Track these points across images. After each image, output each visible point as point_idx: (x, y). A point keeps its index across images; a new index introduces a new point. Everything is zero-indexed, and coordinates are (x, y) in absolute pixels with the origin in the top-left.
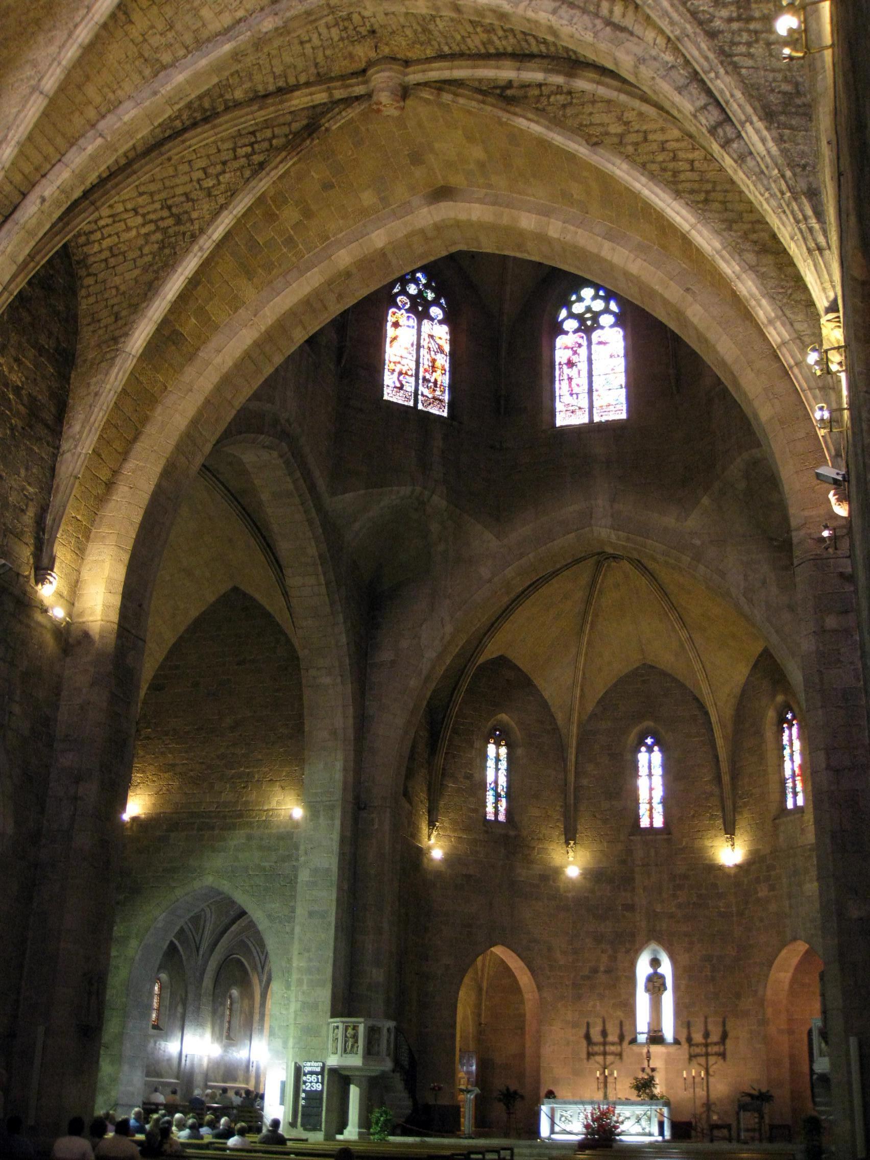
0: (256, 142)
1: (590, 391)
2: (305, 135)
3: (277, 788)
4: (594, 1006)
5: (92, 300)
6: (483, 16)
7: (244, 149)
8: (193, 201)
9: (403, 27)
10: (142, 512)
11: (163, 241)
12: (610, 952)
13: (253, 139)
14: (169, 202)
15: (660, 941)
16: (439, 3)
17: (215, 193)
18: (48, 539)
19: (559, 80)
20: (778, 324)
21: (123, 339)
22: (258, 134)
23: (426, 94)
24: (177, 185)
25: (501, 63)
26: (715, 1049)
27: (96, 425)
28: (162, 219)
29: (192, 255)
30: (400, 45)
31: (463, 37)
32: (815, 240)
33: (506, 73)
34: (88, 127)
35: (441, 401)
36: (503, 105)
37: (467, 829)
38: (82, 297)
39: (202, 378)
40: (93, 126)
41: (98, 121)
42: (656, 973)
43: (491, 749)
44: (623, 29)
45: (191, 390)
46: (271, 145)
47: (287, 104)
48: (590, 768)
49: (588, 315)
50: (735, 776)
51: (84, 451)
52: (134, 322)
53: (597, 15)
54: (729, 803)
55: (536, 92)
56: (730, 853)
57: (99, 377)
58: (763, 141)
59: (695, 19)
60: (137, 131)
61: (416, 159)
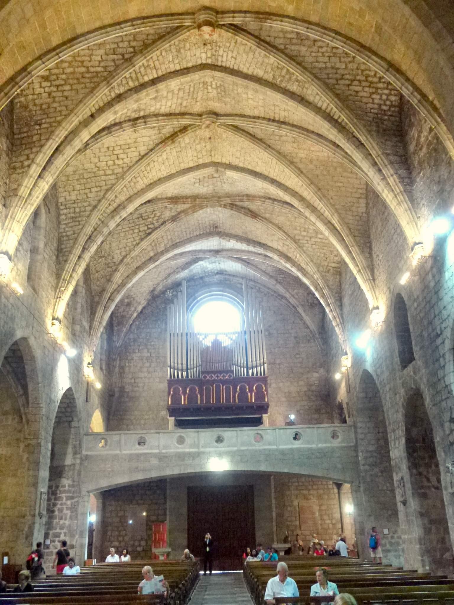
31: (161, 54)
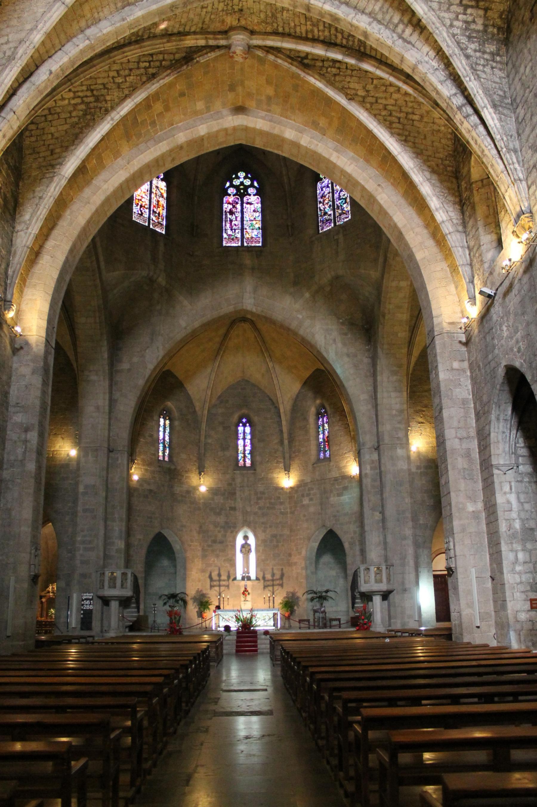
0: (152, 61)
1: (242, 229)
2: (183, 62)
3: (59, 439)
4: (214, 561)
5: (33, 139)
6: (323, 17)
7: (145, 64)
8: (108, 89)
9: (261, 11)
10: (58, 272)
11: (86, 110)
12: (222, 532)
13: (151, 59)
14: (92, 87)
15: (249, 526)
16: (298, 4)
17: (123, 87)
18: (10, 284)
19: (352, 61)
20: (441, 211)
21: (58, 167)
22: (154, 57)
23: (260, 53)
24: (99, 78)
25: (315, 44)
26: (278, 582)
27: (41, 217)
28: (87, 96)
29: (106, 122)
30: (253, 22)
31: (295, 25)
32: (517, 175)
33: (319, 51)
34: (79, 31)
35: (162, 225)
36: (303, 68)
37: (150, 464)
38: (27, 137)
39: (95, 197)
40: (82, 31)
41: (85, 29)
42: (246, 543)
43: (162, 421)
44: (409, 43)
45: (89, 203)
46: (161, 64)
47: (184, 42)
48: (212, 433)
49: (242, 187)
50: (291, 440)
51: (33, 232)
52: (66, 157)
53: (394, 31)
54: (287, 455)
55: (321, 64)
56: (287, 481)
57: (42, 188)
58: (493, 119)
59: (459, 46)
60: (107, 41)
61: (232, 88)
